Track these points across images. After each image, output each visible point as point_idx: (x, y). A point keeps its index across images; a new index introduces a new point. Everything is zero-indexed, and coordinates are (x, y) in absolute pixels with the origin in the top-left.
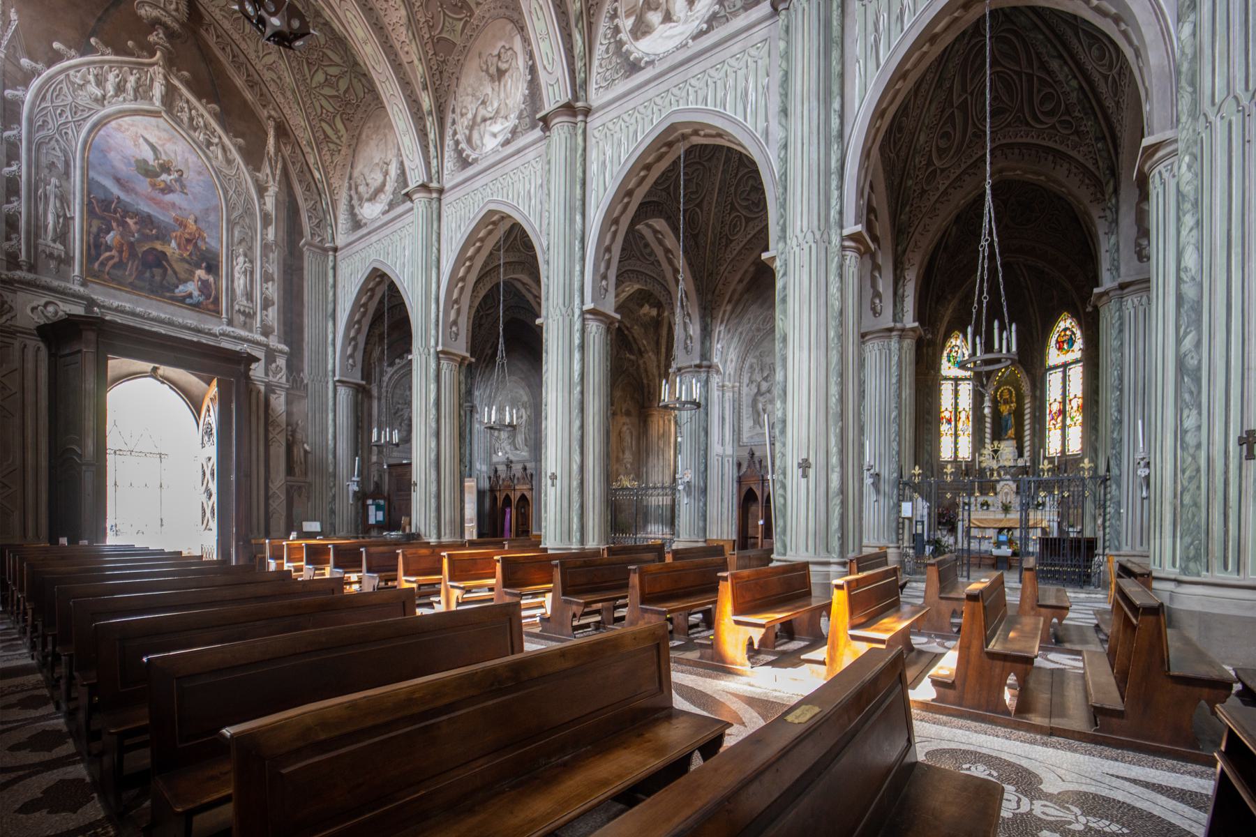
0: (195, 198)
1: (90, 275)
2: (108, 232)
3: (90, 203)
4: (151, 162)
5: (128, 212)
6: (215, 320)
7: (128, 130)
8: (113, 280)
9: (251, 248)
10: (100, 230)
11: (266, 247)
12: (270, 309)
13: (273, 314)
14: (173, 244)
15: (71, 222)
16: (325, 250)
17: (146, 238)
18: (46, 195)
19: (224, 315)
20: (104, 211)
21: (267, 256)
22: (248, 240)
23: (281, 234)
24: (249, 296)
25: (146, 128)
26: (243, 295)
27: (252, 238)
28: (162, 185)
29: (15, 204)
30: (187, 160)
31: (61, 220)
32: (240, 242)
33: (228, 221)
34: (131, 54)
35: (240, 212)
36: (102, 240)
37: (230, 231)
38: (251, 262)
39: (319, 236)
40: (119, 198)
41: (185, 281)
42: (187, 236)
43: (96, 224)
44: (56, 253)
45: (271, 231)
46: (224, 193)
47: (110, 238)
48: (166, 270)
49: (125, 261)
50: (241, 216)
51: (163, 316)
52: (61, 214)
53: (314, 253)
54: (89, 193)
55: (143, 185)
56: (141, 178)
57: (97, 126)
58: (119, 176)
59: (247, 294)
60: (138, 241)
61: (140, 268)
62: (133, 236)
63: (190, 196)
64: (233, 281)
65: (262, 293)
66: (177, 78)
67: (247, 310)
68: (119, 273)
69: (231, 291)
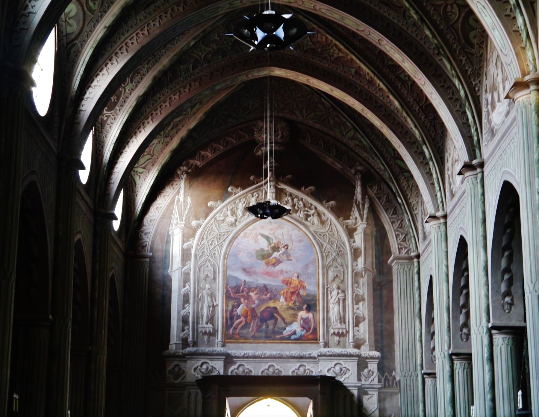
0: (297, 261)
1: (228, 338)
2: (238, 306)
3: (228, 291)
5: (251, 288)
6: (314, 346)
7: (251, 234)
8: (241, 337)
9: (343, 281)
11: (356, 275)
12: (361, 325)
14: (282, 299)
15: (216, 308)
16: (411, 259)
17: (262, 301)
18: (203, 297)
20: (236, 293)
21: (357, 282)
22: (341, 275)
23: (369, 260)
25: (262, 227)
26: (336, 320)
27: (344, 273)
28: (274, 261)
29: (187, 308)
30: (291, 236)
31: (211, 309)
32: (334, 280)
33: (323, 267)
34: (253, 184)
35: (333, 256)
36: (235, 313)
38: (344, 292)
39: (405, 248)
40: (245, 281)
41: (291, 323)
42: (292, 290)
43: (231, 303)
44: (208, 331)
45: (361, 262)
46: (320, 248)
47: (239, 311)
48: (276, 319)
49: (249, 322)
50: (334, 259)
51: (274, 353)
52: (211, 305)
53: (402, 264)
55: (261, 266)
56: (259, 261)
57: (232, 241)
58: (245, 267)
59: (340, 318)
60: (258, 306)
61: (259, 323)
62: (254, 303)
63: (294, 261)
64: (328, 312)
65: (354, 314)
67: (341, 332)
68: (245, 331)
69: (327, 320)
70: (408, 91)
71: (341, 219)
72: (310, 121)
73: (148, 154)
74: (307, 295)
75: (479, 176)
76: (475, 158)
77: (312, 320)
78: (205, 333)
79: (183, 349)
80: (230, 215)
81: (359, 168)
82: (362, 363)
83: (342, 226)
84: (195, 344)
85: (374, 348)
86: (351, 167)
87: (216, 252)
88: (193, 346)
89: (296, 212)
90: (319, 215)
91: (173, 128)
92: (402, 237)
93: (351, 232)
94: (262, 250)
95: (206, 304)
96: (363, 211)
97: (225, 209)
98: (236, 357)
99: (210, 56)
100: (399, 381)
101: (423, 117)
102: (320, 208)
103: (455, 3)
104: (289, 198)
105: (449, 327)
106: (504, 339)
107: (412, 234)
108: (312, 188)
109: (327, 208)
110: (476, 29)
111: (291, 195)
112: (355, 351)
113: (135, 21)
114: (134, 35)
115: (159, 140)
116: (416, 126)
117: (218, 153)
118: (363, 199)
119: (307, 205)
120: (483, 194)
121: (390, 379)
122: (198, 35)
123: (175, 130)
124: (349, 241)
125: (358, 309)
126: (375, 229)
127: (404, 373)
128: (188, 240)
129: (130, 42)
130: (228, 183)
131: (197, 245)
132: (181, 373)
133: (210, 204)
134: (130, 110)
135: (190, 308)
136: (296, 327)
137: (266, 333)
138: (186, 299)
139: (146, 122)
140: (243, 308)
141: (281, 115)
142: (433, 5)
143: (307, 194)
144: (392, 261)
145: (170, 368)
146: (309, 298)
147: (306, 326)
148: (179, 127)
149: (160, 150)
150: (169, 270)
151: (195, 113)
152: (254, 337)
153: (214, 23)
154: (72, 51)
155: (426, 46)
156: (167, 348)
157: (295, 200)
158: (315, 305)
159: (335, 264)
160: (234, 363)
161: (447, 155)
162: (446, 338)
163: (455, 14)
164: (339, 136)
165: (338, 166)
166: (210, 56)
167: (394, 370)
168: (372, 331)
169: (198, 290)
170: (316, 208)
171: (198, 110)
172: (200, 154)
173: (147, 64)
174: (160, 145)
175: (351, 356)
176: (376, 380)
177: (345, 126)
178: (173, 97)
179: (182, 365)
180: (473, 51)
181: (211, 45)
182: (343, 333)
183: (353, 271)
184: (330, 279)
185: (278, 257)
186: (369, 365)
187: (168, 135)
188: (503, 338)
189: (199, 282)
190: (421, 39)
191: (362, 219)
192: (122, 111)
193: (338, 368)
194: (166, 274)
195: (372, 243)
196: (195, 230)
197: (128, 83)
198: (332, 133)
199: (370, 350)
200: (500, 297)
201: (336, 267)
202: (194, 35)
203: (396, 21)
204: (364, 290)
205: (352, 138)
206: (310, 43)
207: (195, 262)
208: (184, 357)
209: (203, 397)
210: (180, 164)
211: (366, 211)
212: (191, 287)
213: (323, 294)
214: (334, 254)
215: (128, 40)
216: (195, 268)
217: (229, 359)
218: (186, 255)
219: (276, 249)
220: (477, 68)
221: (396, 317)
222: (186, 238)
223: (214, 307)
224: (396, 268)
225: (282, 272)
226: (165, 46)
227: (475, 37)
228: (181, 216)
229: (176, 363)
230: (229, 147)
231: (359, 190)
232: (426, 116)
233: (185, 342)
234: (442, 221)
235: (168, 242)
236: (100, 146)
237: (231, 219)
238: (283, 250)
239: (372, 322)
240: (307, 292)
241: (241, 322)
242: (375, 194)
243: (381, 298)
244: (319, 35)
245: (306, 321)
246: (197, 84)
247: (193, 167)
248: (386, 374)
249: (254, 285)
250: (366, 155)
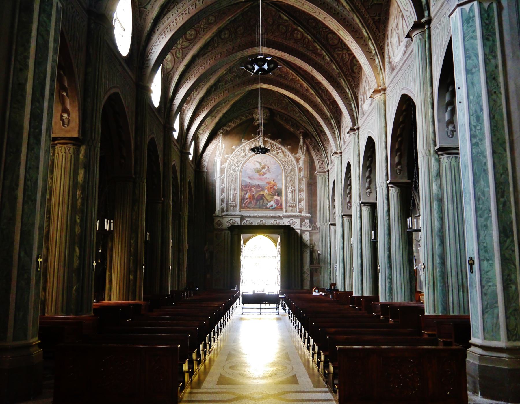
1: (242, 208)
2: (247, 194)
3: (242, 187)
4: (259, 168)
10: (244, 194)
11: (300, 180)
12: (302, 202)
13: (304, 204)
15: (237, 195)
16: (325, 172)
17: (258, 192)
19: (284, 209)
20: (246, 188)
21: (300, 183)
23: (306, 173)
24: (294, 200)
25: (257, 158)
28: (263, 173)
30: (270, 162)
31: (234, 195)
33: (285, 176)
34: (253, 138)
35: (290, 171)
37: (286, 179)
38: (294, 187)
42: (271, 187)
43: (243, 193)
44: (233, 205)
45: (302, 173)
47: (247, 196)
48: (264, 200)
50: (290, 173)
51: (263, 215)
54: (241, 185)
55: (257, 176)
56: (256, 173)
57: (243, 164)
58: (249, 176)
60: (255, 194)
63: (272, 173)
64: (287, 196)
65: (299, 197)
66: (267, 137)
67: (293, 205)
68: (249, 205)
69: (287, 200)
71: (293, 154)
72: (279, 109)
74: (278, 189)
75: (357, 134)
76: (355, 126)
77: (280, 200)
78: (232, 206)
79: (222, 213)
80: (242, 153)
81: (302, 130)
82: (302, 219)
83: (294, 158)
84: (227, 211)
85: (308, 213)
86: (298, 130)
87: (236, 169)
88: (226, 212)
89: (273, 151)
90: (283, 152)
91: (216, 112)
92: (321, 162)
93: (298, 160)
94: (257, 168)
95: (232, 193)
96: (304, 150)
97: (240, 150)
98: (245, 217)
99: (233, 79)
100: (319, 227)
101: (331, 107)
102: (284, 149)
103: (347, 53)
104: (270, 145)
105: (342, 203)
106: (448, 158)
107: (326, 161)
108: (280, 140)
109: (287, 149)
110: (357, 65)
111: (270, 143)
112: (299, 214)
113: (198, 62)
114: (198, 69)
116: (328, 111)
117: (237, 124)
118: (303, 145)
119: (278, 148)
120: (359, 142)
121: (315, 226)
122: (227, 69)
123: (217, 114)
124: (297, 164)
125: (301, 195)
126: (309, 159)
127: (321, 224)
128: (224, 164)
129: (196, 72)
130: (241, 138)
131: (228, 166)
132: (221, 224)
133: (233, 147)
134: (196, 104)
135: (225, 195)
136: (273, 203)
137: (259, 206)
138: (223, 191)
139: (204, 109)
140: (248, 195)
141: (266, 106)
142: (337, 54)
143: (278, 143)
144: (317, 173)
145: (216, 221)
146: (279, 190)
147: (277, 203)
148: (219, 112)
150: (215, 178)
151: (226, 106)
152: (254, 208)
153: (235, 63)
154: (169, 77)
155: (333, 73)
156: (215, 213)
157: (272, 146)
158: (281, 193)
159: (290, 174)
160: (245, 219)
161: (342, 124)
162: (341, 208)
163: (347, 58)
164: (292, 116)
165: (292, 130)
167: (317, 222)
168: (307, 205)
169: (228, 187)
170: (282, 149)
171: (227, 104)
172: (229, 124)
173: (204, 82)
174: (210, 121)
175: (297, 216)
176: (309, 227)
177: (295, 111)
178: (216, 98)
179: (221, 220)
180: (355, 75)
182: (294, 206)
183: (298, 178)
184: (288, 181)
185: (265, 172)
186: (306, 220)
188: (395, 189)
189: (228, 183)
190: (331, 70)
191: (303, 154)
192: (193, 104)
193: (291, 221)
194: (213, 180)
195: (307, 165)
196: (226, 160)
198: (289, 114)
199: (306, 214)
200: (365, 189)
201: (291, 176)
202: (225, 69)
203: (319, 61)
204: (304, 186)
205: (299, 117)
206: (279, 72)
207: (227, 174)
208: (222, 217)
209: (231, 235)
210: (219, 129)
211: (305, 151)
212: (225, 185)
213: (285, 188)
214: (290, 170)
215: (195, 72)
216: (227, 177)
217: (242, 218)
218: (222, 171)
219: (263, 168)
220: (357, 83)
221: (318, 198)
222: (222, 163)
223: (235, 194)
224: (318, 176)
225: (266, 178)
226: (212, 74)
227: (356, 69)
228: (220, 153)
229: (218, 219)
230: (242, 121)
231: (301, 141)
232: (333, 106)
233: (222, 210)
234: (340, 155)
235: (214, 165)
236: (183, 121)
237: (243, 154)
238: (267, 168)
239: (307, 201)
240: (278, 187)
241: (248, 201)
242: (309, 143)
243: (311, 190)
245: (277, 200)
246: (227, 91)
247: (225, 131)
248: (313, 224)
249: (253, 184)
250: (305, 125)
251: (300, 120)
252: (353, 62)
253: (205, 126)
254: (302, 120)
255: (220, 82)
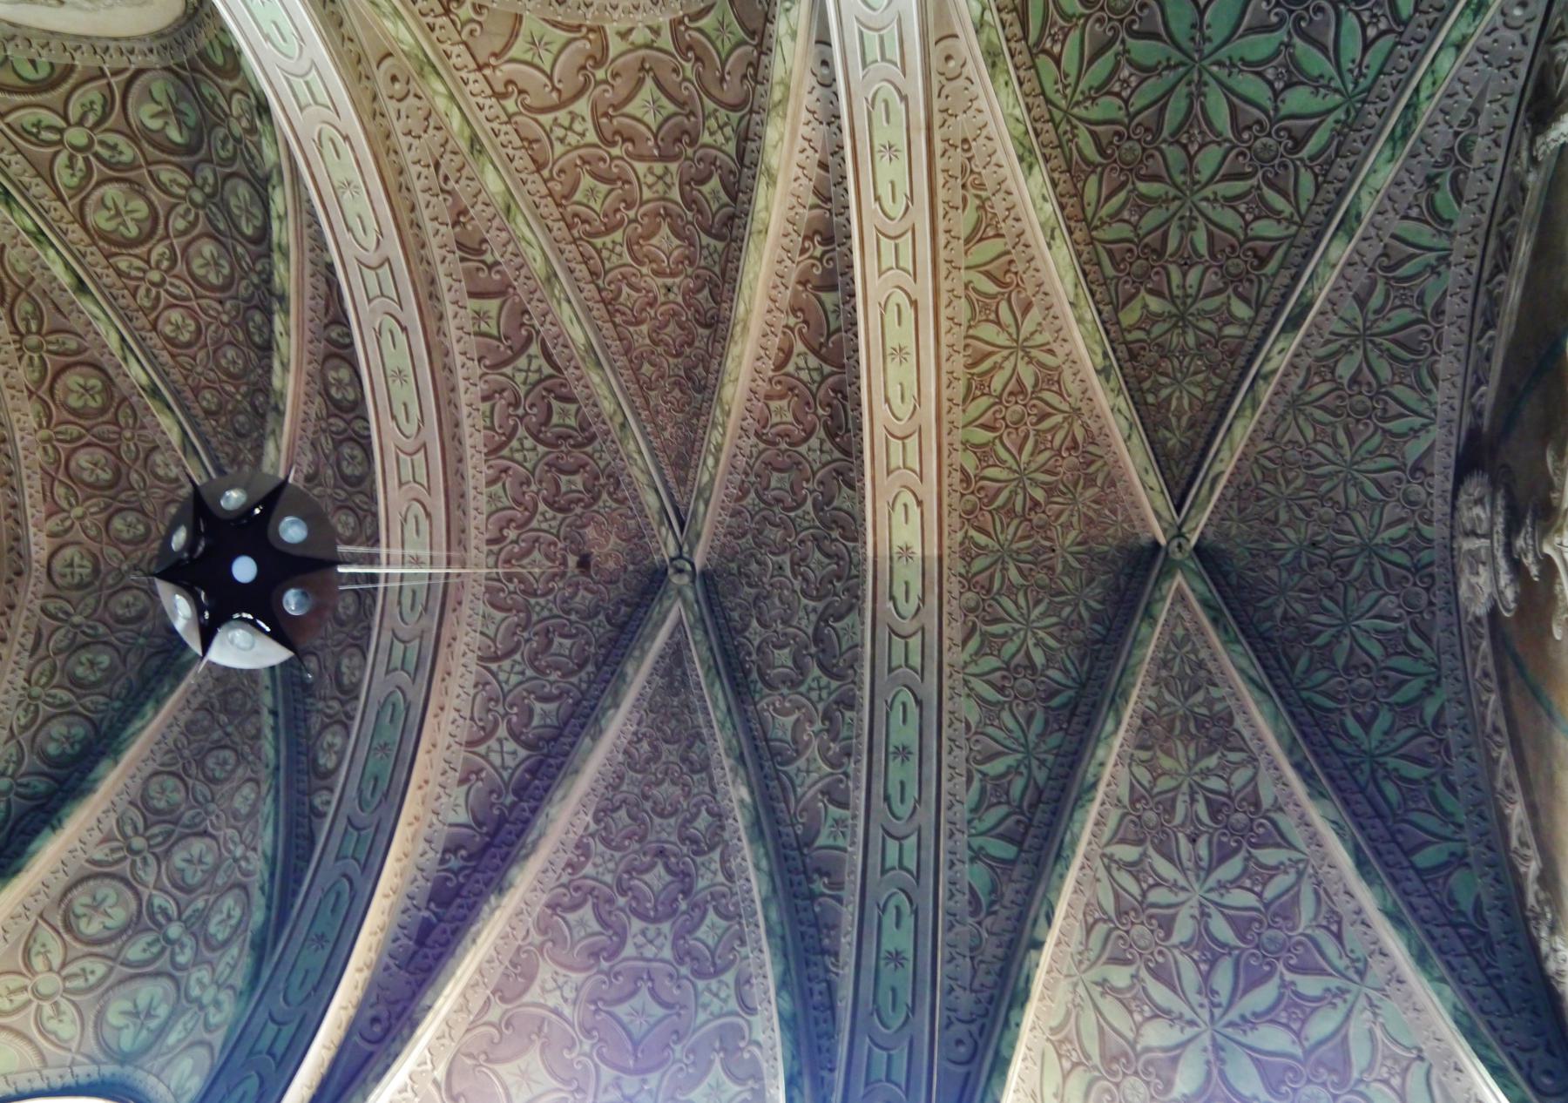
70: (751, 111)
72: (1437, 397)
73: (1406, 1069)
91: (1338, 937)
115: (1363, 1002)
123: (1350, 933)
141: (1440, 508)
149: (1412, 1014)
151: (1315, 840)
166: (835, 747)
174: (1389, 1008)
181: (806, 738)
187: (1360, 965)
197: (748, 1022)
206: (814, 442)
244: (775, 419)
250: (1482, 143)
251: (1458, 195)
252: (50, 75)
253: (1418, 1070)
254: (1454, 178)
255: (818, 833)
